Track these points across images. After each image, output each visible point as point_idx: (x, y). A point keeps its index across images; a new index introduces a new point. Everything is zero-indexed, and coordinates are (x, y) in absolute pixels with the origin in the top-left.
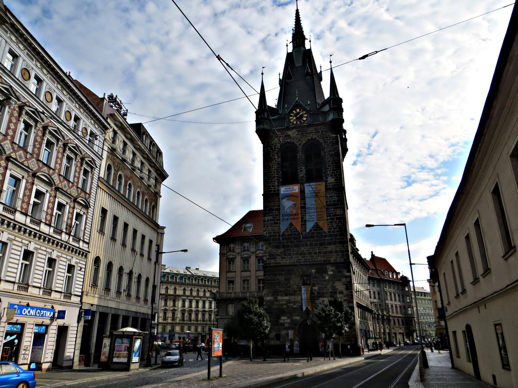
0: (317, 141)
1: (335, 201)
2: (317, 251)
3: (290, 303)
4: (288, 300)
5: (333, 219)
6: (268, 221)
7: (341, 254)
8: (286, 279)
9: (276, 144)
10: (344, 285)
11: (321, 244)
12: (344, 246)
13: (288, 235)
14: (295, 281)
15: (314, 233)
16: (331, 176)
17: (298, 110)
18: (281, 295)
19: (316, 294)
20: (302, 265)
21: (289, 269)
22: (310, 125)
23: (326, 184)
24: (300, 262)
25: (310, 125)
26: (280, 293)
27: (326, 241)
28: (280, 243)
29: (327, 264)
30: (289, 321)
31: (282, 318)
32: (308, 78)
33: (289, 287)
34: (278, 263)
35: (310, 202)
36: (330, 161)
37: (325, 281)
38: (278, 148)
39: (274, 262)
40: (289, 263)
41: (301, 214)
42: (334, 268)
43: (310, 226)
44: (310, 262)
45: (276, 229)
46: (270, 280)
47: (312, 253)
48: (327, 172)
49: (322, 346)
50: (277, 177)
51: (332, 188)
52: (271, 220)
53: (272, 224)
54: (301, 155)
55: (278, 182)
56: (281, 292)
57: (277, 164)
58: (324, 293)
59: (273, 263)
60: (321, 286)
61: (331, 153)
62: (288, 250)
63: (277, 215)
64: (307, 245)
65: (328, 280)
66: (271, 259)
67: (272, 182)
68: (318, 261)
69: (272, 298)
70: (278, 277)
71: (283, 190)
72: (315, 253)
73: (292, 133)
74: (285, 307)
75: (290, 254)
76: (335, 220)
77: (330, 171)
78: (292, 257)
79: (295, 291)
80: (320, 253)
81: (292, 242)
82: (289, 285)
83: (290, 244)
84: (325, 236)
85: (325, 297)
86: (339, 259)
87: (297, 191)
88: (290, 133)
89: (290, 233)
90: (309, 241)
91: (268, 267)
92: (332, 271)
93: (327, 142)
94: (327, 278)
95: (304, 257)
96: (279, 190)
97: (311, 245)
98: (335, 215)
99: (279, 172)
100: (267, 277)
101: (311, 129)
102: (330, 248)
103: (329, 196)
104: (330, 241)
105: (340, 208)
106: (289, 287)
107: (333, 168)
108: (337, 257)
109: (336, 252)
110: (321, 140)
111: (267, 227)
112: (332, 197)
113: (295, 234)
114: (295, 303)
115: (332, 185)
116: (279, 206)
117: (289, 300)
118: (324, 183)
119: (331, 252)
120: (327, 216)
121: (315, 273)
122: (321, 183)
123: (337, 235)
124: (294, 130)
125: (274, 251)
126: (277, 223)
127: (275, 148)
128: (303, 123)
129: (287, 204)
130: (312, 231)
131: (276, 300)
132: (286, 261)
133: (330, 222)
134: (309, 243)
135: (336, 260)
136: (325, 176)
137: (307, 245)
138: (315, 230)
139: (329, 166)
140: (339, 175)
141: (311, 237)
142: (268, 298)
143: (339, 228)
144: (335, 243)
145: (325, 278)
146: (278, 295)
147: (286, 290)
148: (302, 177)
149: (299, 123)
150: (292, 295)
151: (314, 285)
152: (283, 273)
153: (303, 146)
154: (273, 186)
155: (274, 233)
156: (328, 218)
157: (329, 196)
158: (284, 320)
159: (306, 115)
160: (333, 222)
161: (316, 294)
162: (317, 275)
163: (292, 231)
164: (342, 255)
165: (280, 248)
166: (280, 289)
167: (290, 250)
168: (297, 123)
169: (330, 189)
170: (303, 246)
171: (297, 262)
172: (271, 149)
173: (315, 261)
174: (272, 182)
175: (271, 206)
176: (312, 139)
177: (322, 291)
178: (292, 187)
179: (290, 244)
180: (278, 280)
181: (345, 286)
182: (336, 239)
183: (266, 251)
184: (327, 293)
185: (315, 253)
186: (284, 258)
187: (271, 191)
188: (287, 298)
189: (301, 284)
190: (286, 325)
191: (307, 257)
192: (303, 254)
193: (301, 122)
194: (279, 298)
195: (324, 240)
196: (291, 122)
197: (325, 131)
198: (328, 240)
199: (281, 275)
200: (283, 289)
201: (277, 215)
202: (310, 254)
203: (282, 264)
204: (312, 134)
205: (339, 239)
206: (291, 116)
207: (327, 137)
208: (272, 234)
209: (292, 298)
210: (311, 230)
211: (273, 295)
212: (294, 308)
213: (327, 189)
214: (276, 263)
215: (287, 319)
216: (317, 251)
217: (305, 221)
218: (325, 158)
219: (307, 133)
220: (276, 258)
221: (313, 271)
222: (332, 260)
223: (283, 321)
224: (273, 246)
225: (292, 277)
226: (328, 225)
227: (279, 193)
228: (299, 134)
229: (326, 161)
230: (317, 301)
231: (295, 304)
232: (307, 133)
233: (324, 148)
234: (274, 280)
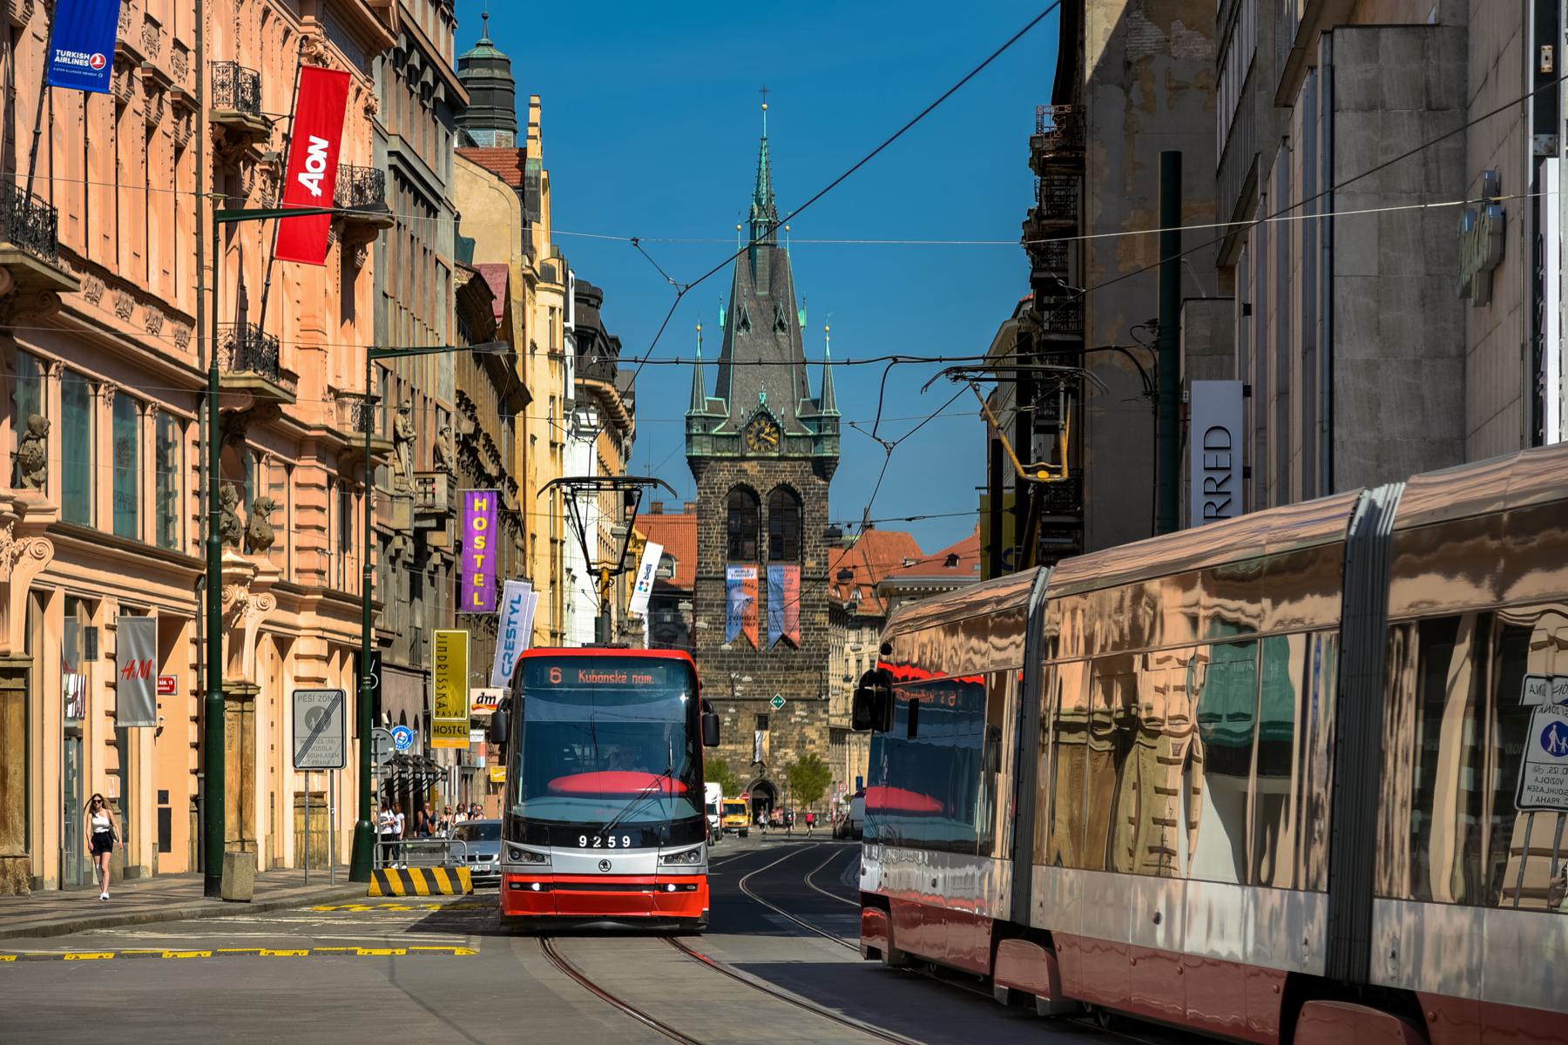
14: (747, 723)
22: (780, 459)
25: (780, 459)
32: (779, 333)
73: (751, 468)
87: (755, 577)
88: (746, 465)
96: (725, 572)
97: (772, 668)
101: (782, 465)
110: (799, 489)
124: (754, 463)
129: (739, 598)
151: (773, 730)
169: (808, 579)
188: (732, 747)
202: (770, 682)
204: (786, 474)
209: (740, 748)
222: (803, 694)
227: (724, 579)
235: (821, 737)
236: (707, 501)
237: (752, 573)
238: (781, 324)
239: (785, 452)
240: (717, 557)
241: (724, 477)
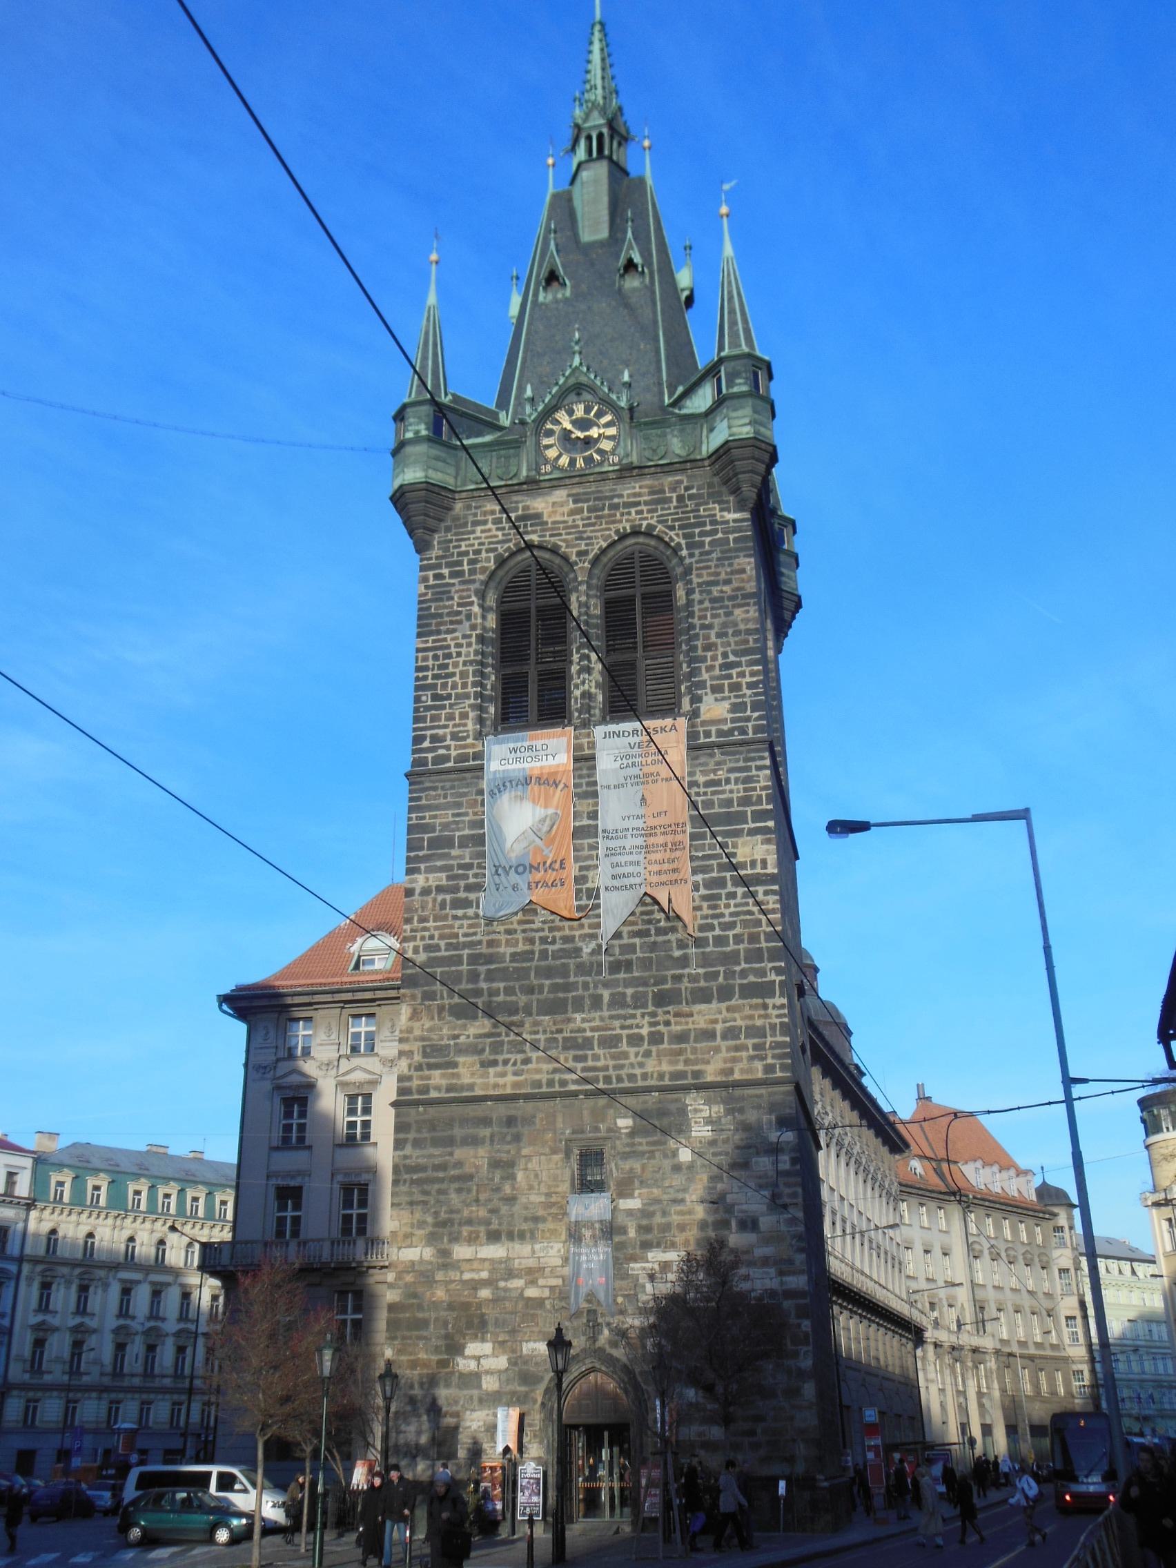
0: (659, 538)
1: (729, 803)
2: (645, 1031)
3: (511, 1274)
4: (501, 1262)
5: (721, 883)
6: (426, 891)
7: (750, 1042)
8: (495, 1164)
9: (478, 552)
10: (761, 1187)
11: (662, 999)
12: (765, 1007)
13: (514, 956)
14: (542, 1171)
15: (631, 948)
16: (717, 689)
17: (579, 411)
18: (472, 1240)
19: (632, 1233)
20: (574, 1094)
21: (510, 1117)
22: (628, 471)
23: (692, 725)
24: (563, 1083)
25: (628, 471)
26: (465, 1230)
27: (685, 984)
28: (478, 993)
29: (686, 1089)
30: (502, 1362)
31: (472, 1348)
33: (511, 1200)
34: (463, 1088)
35: (615, 810)
36: (710, 627)
37: (677, 1168)
38: (484, 569)
39: (444, 1082)
40: (516, 1085)
41: (576, 859)
42: (718, 1109)
43: (615, 909)
44: (607, 1079)
45: (461, 929)
46: (422, 1168)
47: (618, 1038)
48: (694, 672)
49: (651, 1484)
50: (477, 695)
51: (720, 746)
52: (440, 889)
53: (443, 905)
54: (584, 603)
55: (481, 721)
56: (469, 1222)
57: (481, 639)
58: (666, 1228)
59: (438, 1088)
60: (655, 1190)
61: (715, 591)
62: (513, 1024)
63: (469, 866)
64: (597, 1002)
65: (691, 1166)
66: (431, 1067)
67: (450, 717)
68: (645, 1076)
69: (428, 1253)
70: (459, 1153)
71: (504, 756)
72: (635, 1040)
73: (552, 507)
74: (485, 1293)
75: (518, 1047)
76: (730, 888)
77: (710, 669)
78: (527, 1061)
79: (536, 1219)
80: (656, 1038)
81: (530, 990)
82: (507, 1189)
83: (522, 999)
84: (684, 961)
85: (673, 1245)
86: (744, 1064)
89: (521, 947)
90: (606, 985)
91: (417, 1103)
92: (709, 1121)
93: (702, 544)
94: (685, 1155)
95: (583, 1058)
96: (479, 756)
98: (734, 867)
99: (482, 675)
100: (408, 1150)
102: (703, 1015)
103: (701, 779)
104: (702, 984)
105: (752, 832)
106: (511, 1200)
107: (725, 655)
108: (734, 1060)
109: (730, 1033)
110: (676, 538)
111: (423, 920)
112: (716, 783)
113: (544, 954)
114: (532, 1275)
115: (720, 733)
116: (481, 824)
117: (508, 1259)
118: (682, 722)
119: (709, 1035)
120: (695, 871)
121: (633, 1133)
122: (668, 722)
123: (733, 958)
124: (560, 495)
125: (445, 1031)
126: (466, 904)
127: (472, 572)
128: (601, 464)
130: (625, 941)
131: (446, 1261)
132: (503, 1080)
133: (704, 898)
134: (606, 994)
135: (731, 1071)
136: (689, 689)
137: (597, 1002)
138: (639, 934)
139: (708, 647)
140: (750, 686)
141: (616, 967)
142: (411, 1254)
143: (745, 924)
144: (725, 994)
145: (675, 1154)
146: (455, 1239)
147: (492, 1211)
148: (587, 695)
149: (580, 463)
150: (522, 1236)
151: (625, 1189)
152: (485, 1132)
153: (595, 561)
154: (455, 737)
155: (449, 946)
156: (699, 878)
157: (701, 779)
158: (478, 1359)
159: (612, 431)
160: (718, 897)
161: (632, 1233)
162: (642, 1142)
163: (532, 941)
164: (756, 1047)
165: (475, 1018)
166: (466, 1213)
167: (521, 1024)
168: (572, 462)
170: (578, 1006)
171: (550, 1083)
172: (453, 575)
173: (632, 1077)
174: (450, 717)
175: (445, 826)
176: (636, 532)
177: (658, 1219)
178: (539, 743)
179: (522, 999)
180: (459, 1164)
181: (766, 1193)
182: (730, 974)
183: (410, 1030)
184: (682, 1228)
185: (635, 1040)
186: (494, 1063)
187: (446, 758)
189: (565, 1187)
190: (489, 1384)
191: (596, 1058)
192: (578, 1045)
193: (589, 460)
194: (462, 1252)
195: (677, 978)
196: (546, 462)
197: (691, 497)
198: (694, 979)
199: (474, 1141)
200: (483, 1213)
201: (469, 866)
202: (610, 1042)
203: (479, 1092)
204: (638, 509)
205: (743, 974)
206: (550, 433)
207: (704, 524)
208: (443, 953)
209: (521, 1253)
210: (617, 935)
211: (432, 1239)
212: (529, 1299)
213: (694, 748)
214: (448, 1090)
215: (494, 1355)
216: (645, 1031)
217: (594, 894)
218: (691, 615)
219: (615, 507)
220: (455, 1065)
221: (625, 1123)
223: (472, 1365)
224: (441, 1009)
225: (525, 1152)
226: (696, 909)
228: (581, 511)
229: (692, 627)
230: (636, 1268)
231: (533, 1283)
232: (615, 507)
233: (688, 571)
234: (443, 1167)
235: (776, 1204)
236: (441, 593)
237: (551, 749)
238: (630, 265)
239: (634, 459)
240: (461, 721)
241: (484, 536)
